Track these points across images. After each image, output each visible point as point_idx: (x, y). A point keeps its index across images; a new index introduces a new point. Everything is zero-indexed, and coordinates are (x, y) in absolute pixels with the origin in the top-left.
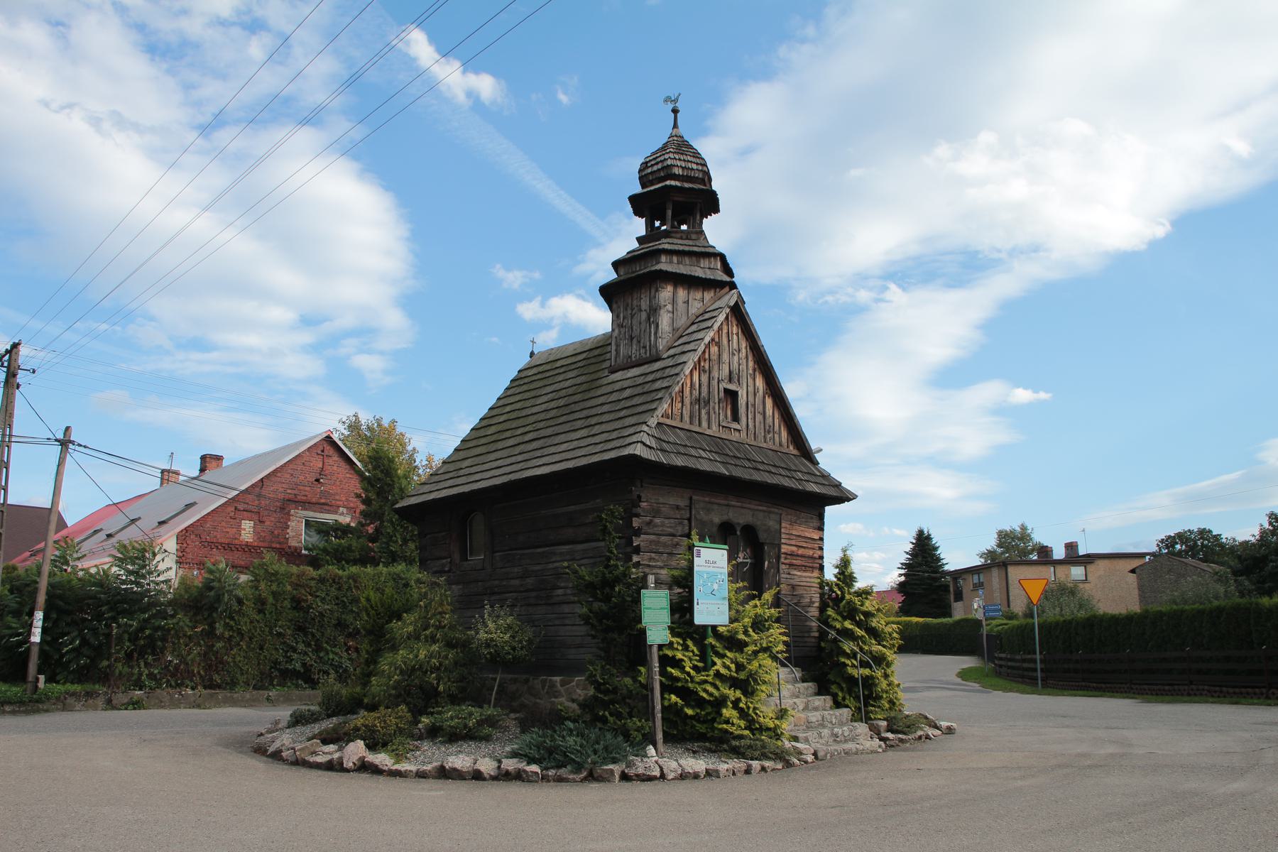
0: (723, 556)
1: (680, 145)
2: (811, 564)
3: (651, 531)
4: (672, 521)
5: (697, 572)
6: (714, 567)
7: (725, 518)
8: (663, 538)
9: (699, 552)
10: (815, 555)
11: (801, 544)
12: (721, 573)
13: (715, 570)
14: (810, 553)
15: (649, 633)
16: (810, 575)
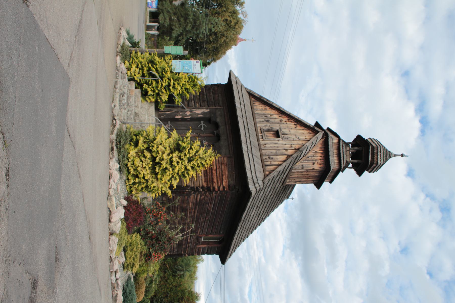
0: (199, 71)
1: (388, 155)
2: (209, 180)
3: (207, 92)
4: (213, 100)
5: (191, 61)
6: (194, 67)
7: (220, 124)
8: (205, 96)
9: (198, 62)
10: (214, 184)
11: (218, 172)
12: (192, 70)
13: (193, 69)
14: (215, 180)
15: (168, 47)
16: (203, 181)
